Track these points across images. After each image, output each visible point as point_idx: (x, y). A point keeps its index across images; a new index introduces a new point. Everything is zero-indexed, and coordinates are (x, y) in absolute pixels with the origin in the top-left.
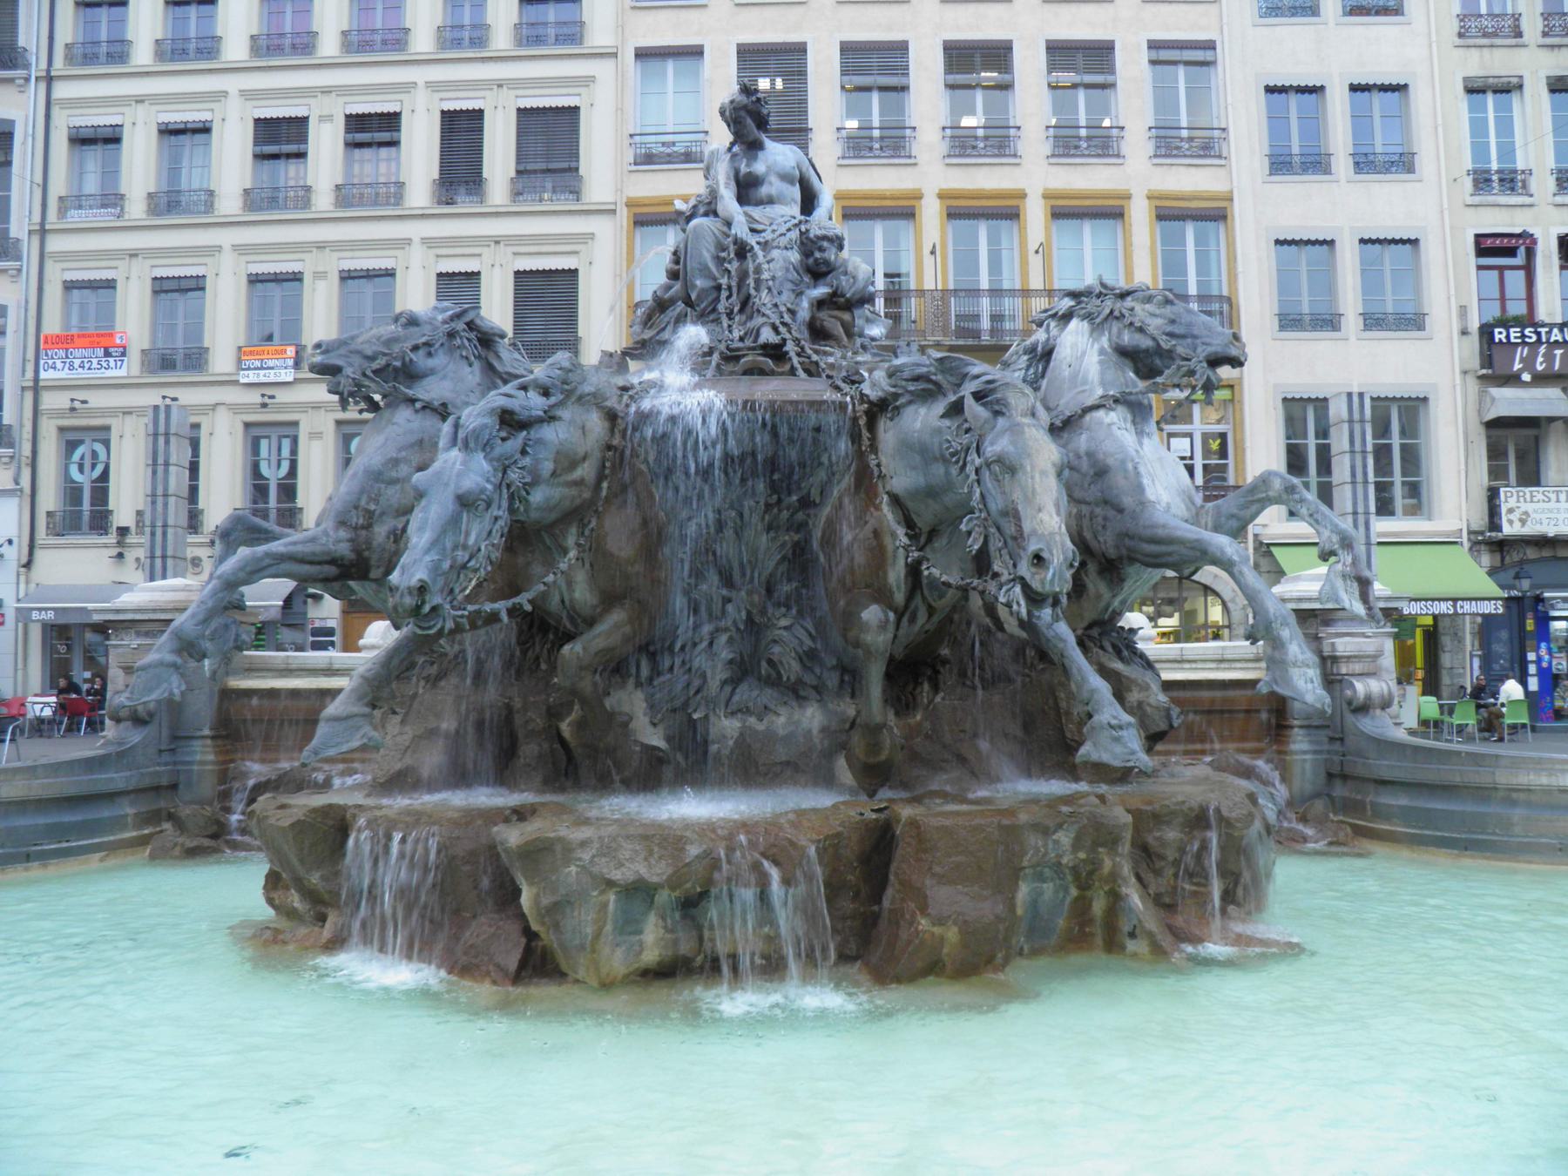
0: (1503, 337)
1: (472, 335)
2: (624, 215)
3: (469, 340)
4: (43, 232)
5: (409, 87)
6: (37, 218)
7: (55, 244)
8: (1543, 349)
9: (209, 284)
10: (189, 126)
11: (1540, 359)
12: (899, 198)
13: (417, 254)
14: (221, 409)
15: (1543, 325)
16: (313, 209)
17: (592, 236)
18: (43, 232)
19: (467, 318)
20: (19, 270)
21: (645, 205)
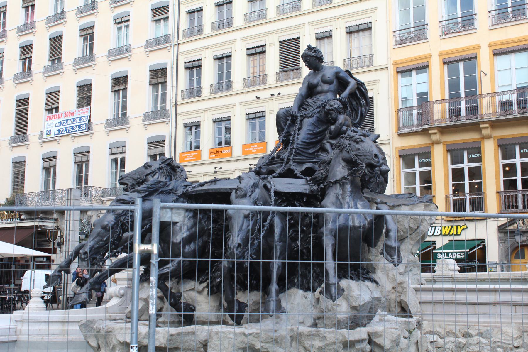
1: (168, 168)
2: (392, 70)
3: (166, 170)
4: (176, 105)
5: (302, 26)
6: (174, 100)
7: (180, 109)
9: (232, 119)
10: (224, 55)
12: (521, 41)
16: (268, 84)
17: (378, 81)
18: (176, 105)
19: (168, 162)
20: (169, 121)
21: (401, 63)
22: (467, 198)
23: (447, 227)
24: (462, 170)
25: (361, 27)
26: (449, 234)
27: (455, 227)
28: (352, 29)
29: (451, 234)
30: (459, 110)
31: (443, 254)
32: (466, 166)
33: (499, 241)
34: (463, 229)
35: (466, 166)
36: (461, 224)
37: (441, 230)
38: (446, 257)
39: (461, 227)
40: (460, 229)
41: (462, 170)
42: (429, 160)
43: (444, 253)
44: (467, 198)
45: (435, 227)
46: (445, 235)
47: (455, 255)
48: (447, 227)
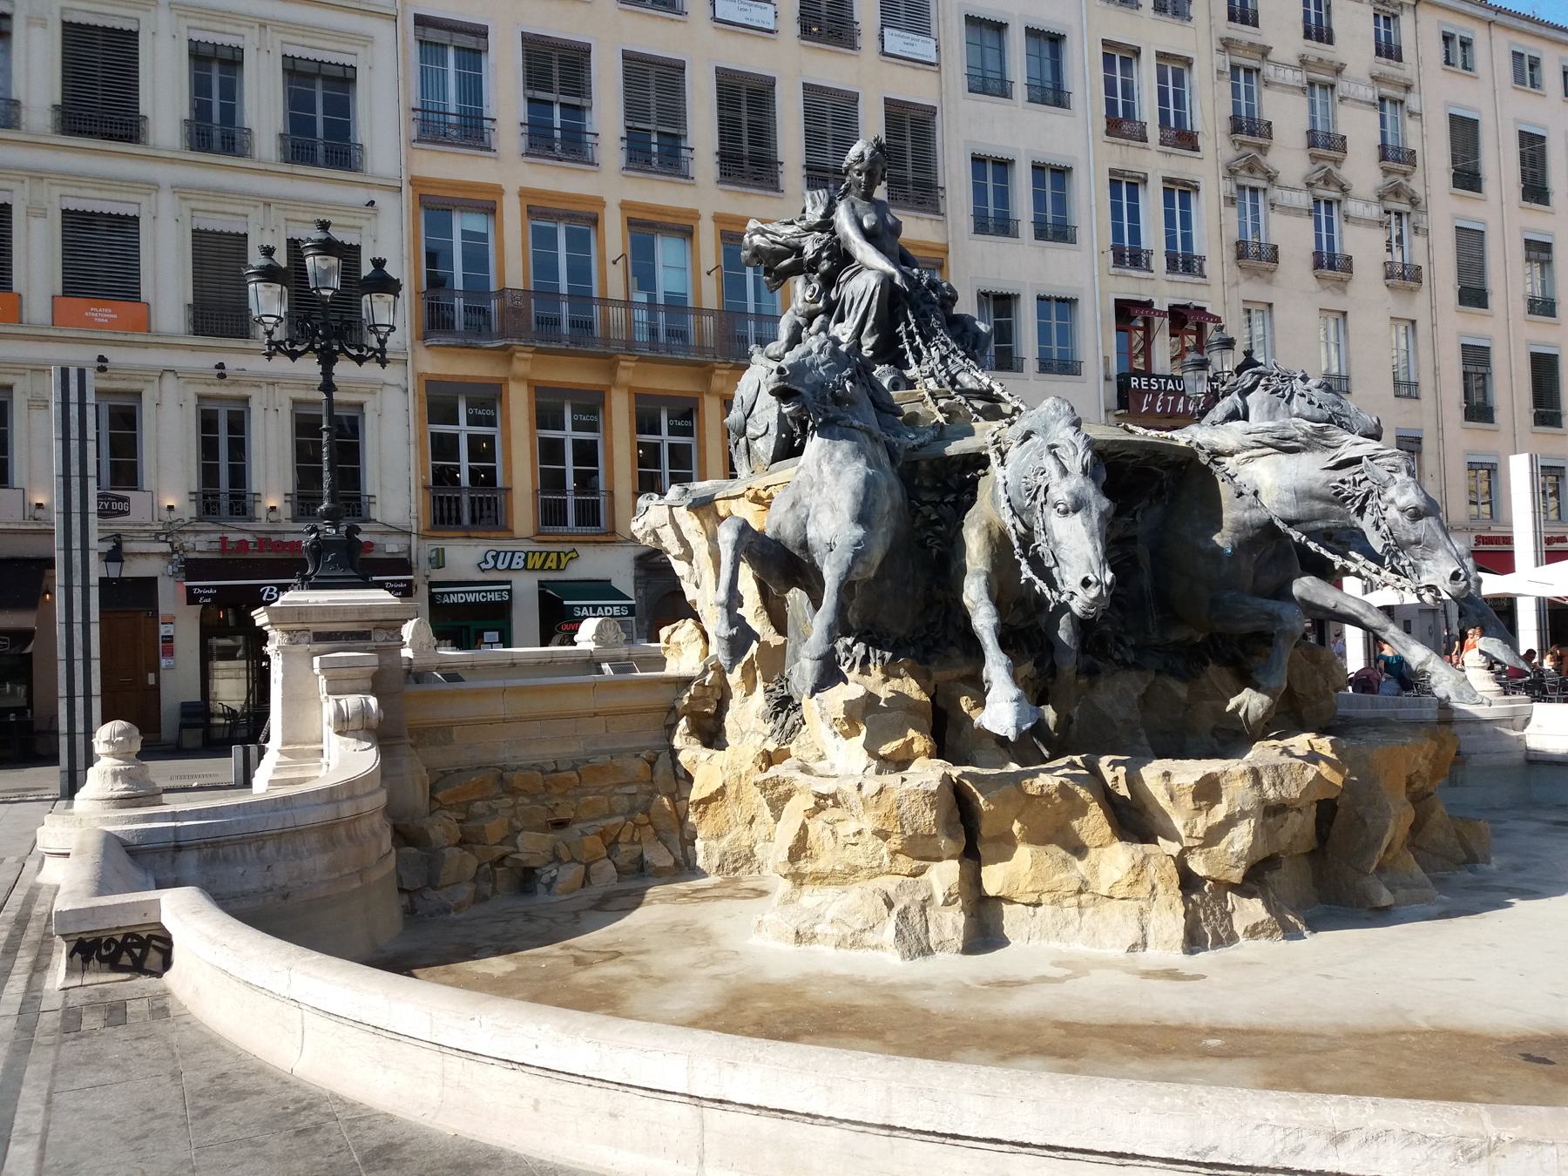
0: (1136, 384)
8: (1161, 397)
11: (1159, 404)
13: (166, 203)
14: (169, 380)
15: (1162, 377)
22: (571, 500)
23: (537, 554)
24: (560, 443)
25: (326, 70)
26: (542, 568)
27: (554, 556)
28: (300, 66)
29: (546, 567)
30: (556, 322)
31: (585, 609)
32: (569, 435)
33: (635, 583)
34: (571, 558)
35: (569, 435)
36: (567, 548)
37: (526, 560)
38: (591, 614)
39: (566, 555)
40: (564, 560)
41: (560, 443)
42: (593, 418)
43: (588, 606)
44: (571, 500)
45: (513, 553)
46: (533, 569)
47: (609, 611)
48: (537, 554)
